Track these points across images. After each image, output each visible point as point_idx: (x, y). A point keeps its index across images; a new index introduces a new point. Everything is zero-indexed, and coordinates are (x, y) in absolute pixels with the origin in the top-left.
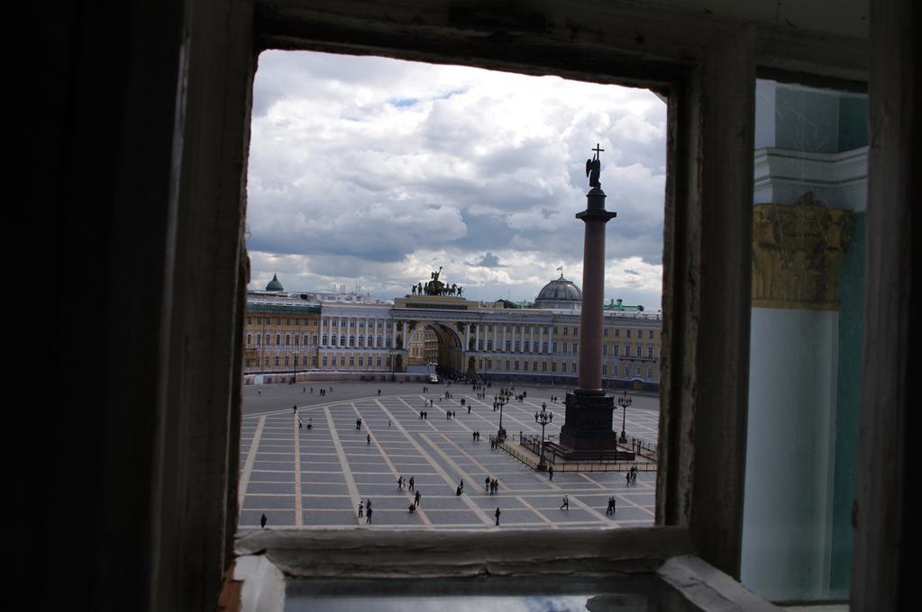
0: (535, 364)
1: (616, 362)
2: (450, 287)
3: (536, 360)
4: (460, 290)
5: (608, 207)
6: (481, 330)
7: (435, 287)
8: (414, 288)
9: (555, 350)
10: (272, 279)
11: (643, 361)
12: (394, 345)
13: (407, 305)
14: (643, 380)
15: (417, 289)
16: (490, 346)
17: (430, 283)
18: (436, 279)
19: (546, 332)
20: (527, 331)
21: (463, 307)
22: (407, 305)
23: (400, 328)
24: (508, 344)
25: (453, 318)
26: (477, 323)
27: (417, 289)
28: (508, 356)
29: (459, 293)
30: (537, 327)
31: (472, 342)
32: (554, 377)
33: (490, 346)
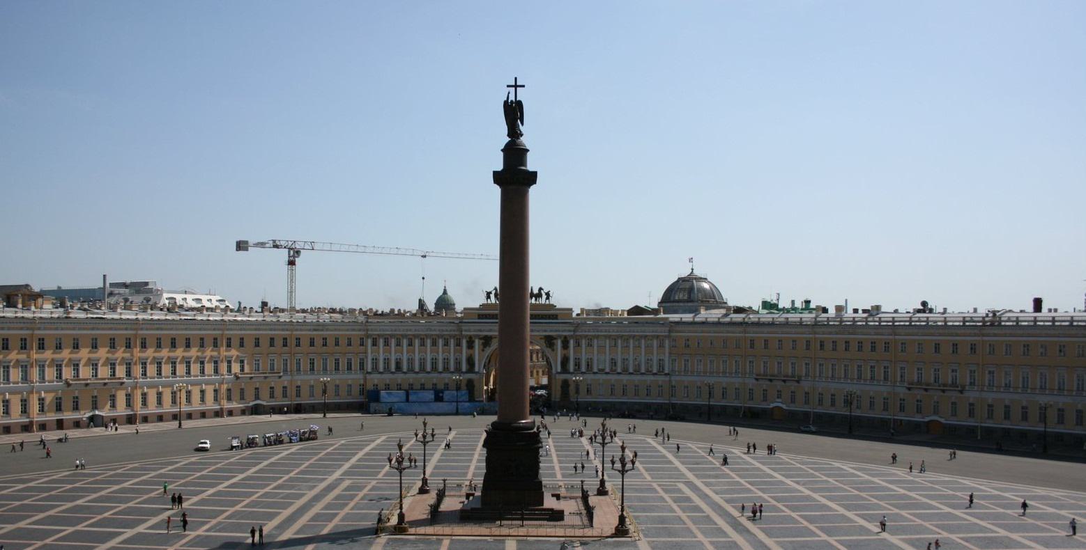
1: (751, 382)
2: (536, 291)
4: (548, 294)
5: (530, 167)
6: (578, 344)
10: (441, 293)
11: (784, 381)
12: (464, 368)
13: (480, 316)
14: (784, 407)
15: (492, 296)
16: (589, 366)
23: (470, 345)
24: (613, 362)
25: (538, 331)
26: (571, 337)
27: (492, 296)
28: (613, 377)
31: (565, 361)
32: (674, 405)
33: (589, 366)
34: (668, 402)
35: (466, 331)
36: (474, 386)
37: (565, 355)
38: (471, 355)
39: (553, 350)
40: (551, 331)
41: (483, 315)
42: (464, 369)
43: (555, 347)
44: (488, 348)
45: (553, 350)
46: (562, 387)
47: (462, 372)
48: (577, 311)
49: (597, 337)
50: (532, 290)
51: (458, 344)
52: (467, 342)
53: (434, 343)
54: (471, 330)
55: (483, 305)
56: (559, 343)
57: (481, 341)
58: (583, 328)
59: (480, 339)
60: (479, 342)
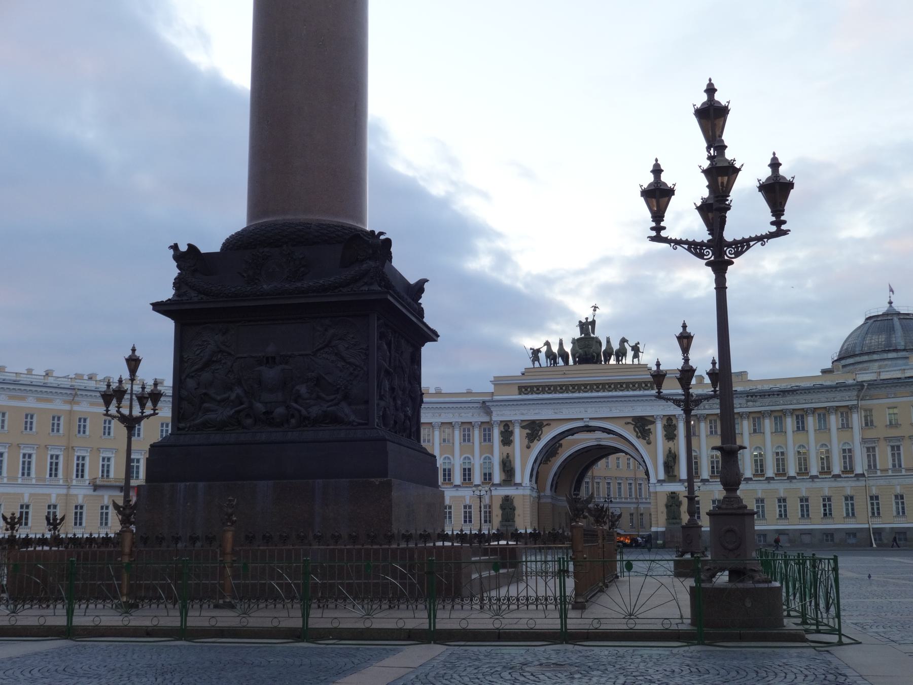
0: (827, 500)
2: (616, 346)
3: (827, 493)
4: (636, 349)
7: (588, 348)
8: (536, 353)
9: (872, 466)
12: (497, 477)
15: (542, 356)
17: (574, 342)
18: (587, 334)
19: (846, 426)
20: (801, 427)
23: (507, 439)
29: (636, 356)
30: (822, 414)
32: (878, 532)
34: (866, 526)
36: (514, 509)
37: (670, 451)
39: (649, 443)
41: (526, 388)
43: (651, 436)
45: (649, 443)
46: (667, 506)
47: (493, 485)
50: (608, 342)
51: (487, 438)
52: (502, 433)
56: (659, 430)
57: (528, 431)
59: (523, 427)
60: (521, 432)
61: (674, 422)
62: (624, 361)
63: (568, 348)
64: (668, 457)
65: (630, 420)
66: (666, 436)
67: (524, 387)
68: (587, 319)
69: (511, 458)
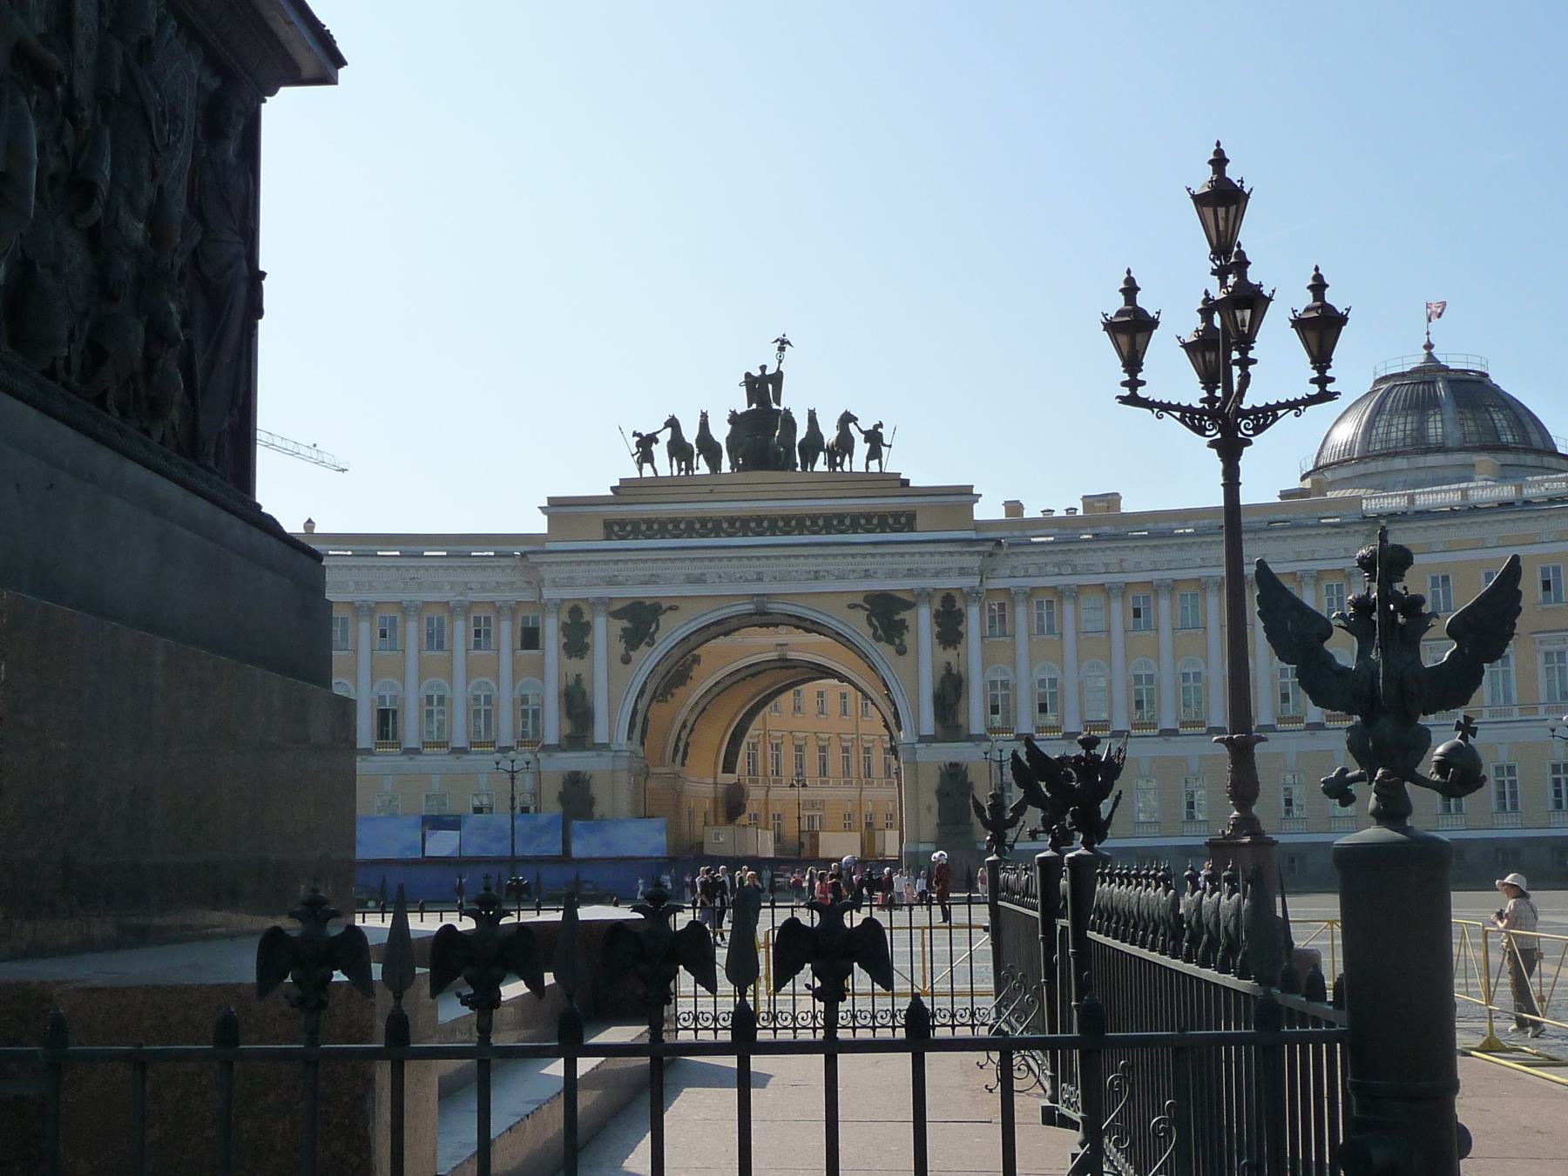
4: (874, 438)
12: (553, 726)
13: (615, 528)
15: (660, 451)
21: (898, 511)
22: (615, 528)
23: (576, 641)
26: (972, 595)
29: (874, 454)
35: (555, 584)
38: (578, 678)
39: (901, 651)
40: (892, 574)
41: (622, 524)
42: (551, 735)
43: (908, 639)
44: (643, 646)
45: (901, 651)
46: (942, 794)
47: (545, 748)
48: (988, 510)
49: (1077, 592)
52: (565, 628)
53: (436, 638)
54: (568, 584)
55: (625, 489)
56: (923, 622)
57: (625, 623)
58: (1014, 561)
59: (616, 615)
61: (959, 604)
62: (846, 468)
63: (721, 432)
64: (943, 680)
65: (859, 600)
66: (939, 636)
67: (616, 522)
68: (763, 368)
69: (586, 686)
